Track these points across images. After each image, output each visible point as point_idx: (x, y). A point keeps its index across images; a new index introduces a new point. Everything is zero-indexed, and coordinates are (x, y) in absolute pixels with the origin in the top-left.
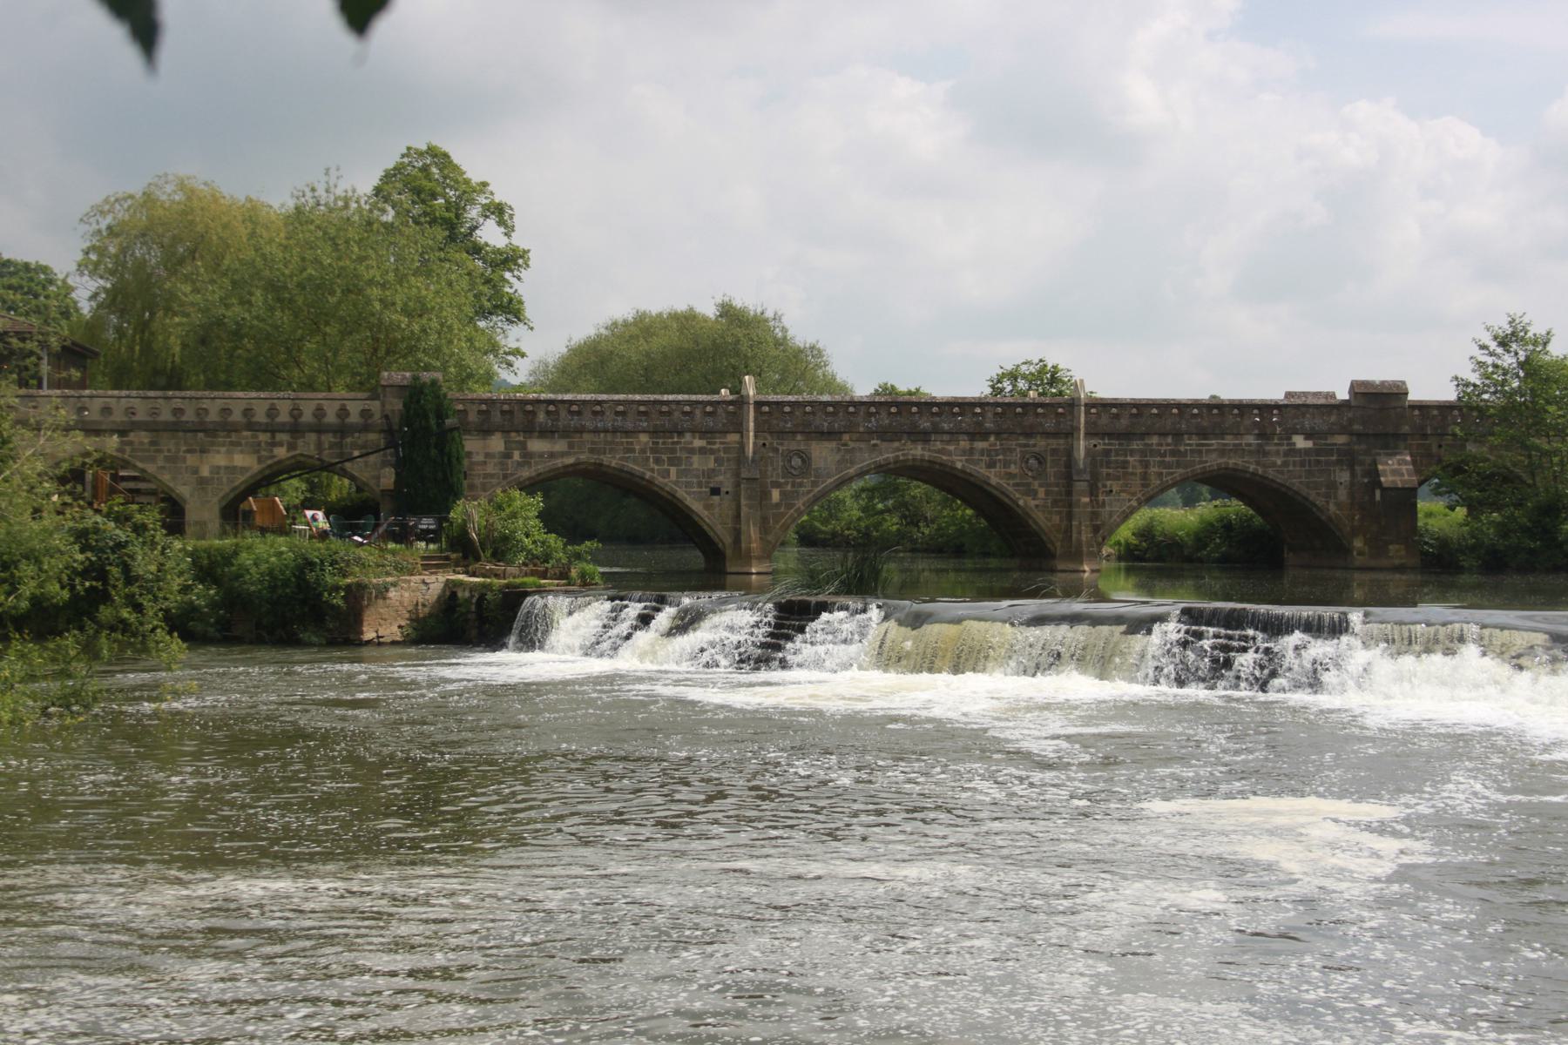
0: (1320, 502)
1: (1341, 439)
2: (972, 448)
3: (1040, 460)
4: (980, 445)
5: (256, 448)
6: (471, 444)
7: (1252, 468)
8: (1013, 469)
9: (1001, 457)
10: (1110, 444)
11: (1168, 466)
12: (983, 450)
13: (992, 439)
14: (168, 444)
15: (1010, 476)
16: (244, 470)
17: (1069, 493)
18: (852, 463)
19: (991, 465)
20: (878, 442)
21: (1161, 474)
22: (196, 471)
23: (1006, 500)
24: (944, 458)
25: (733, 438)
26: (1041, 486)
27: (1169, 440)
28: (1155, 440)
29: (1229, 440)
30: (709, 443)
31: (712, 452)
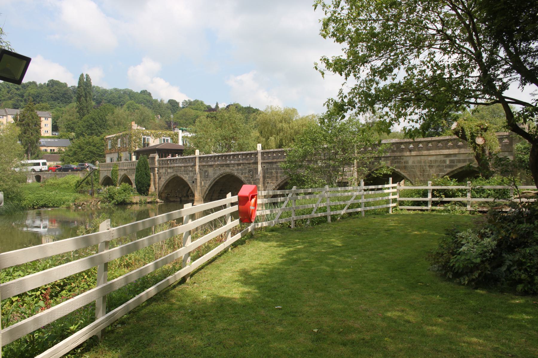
4: (240, 167)
8: (247, 175)
10: (268, 166)
15: (246, 177)
19: (242, 174)
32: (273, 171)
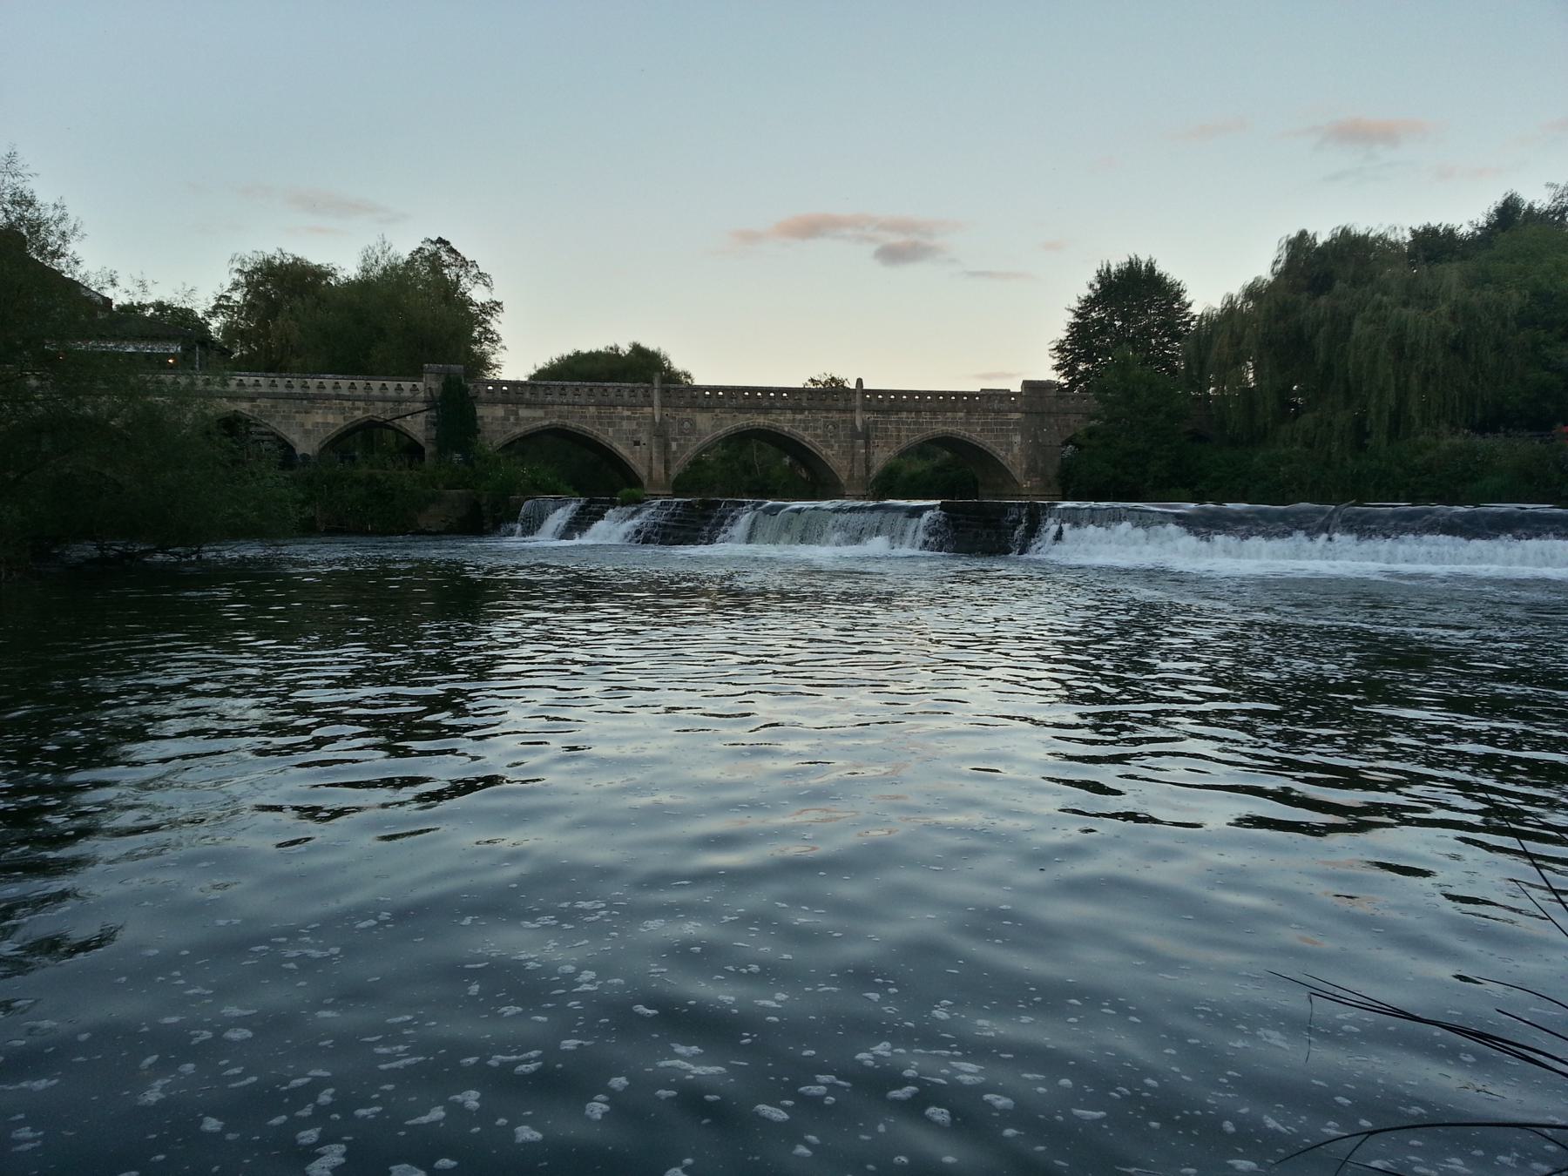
0: (1003, 453)
1: (1016, 416)
3: (835, 426)
4: (799, 417)
5: (342, 410)
6: (481, 411)
7: (962, 432)
8: (819, 432)
11: (913, 431)
12: (800, 420)
13: (806, 413)
14: (284, 407)
15: (817, 436)
16: (334, 425)
17: (852, 447)
19: (806, 429)
20: (737, 414)
21: (908, 436)
22: (303, 425)
23: (815, 451)
24: (777, 424)
25: (648, 410)
26: (835, 442)
27: (913, 415)
28: (904, 415)
29: (949, 414)
30: (633, 413)
31: (635, 419)
32: (889, 426)
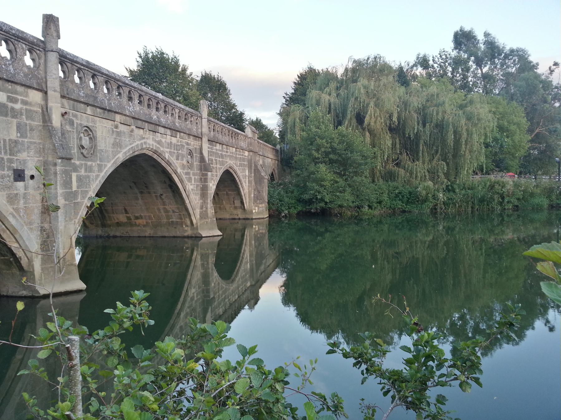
2: (171, 142)
9: (180, 152)
18: (121, 147)
24: (162, 149)
30: (10, 99)
